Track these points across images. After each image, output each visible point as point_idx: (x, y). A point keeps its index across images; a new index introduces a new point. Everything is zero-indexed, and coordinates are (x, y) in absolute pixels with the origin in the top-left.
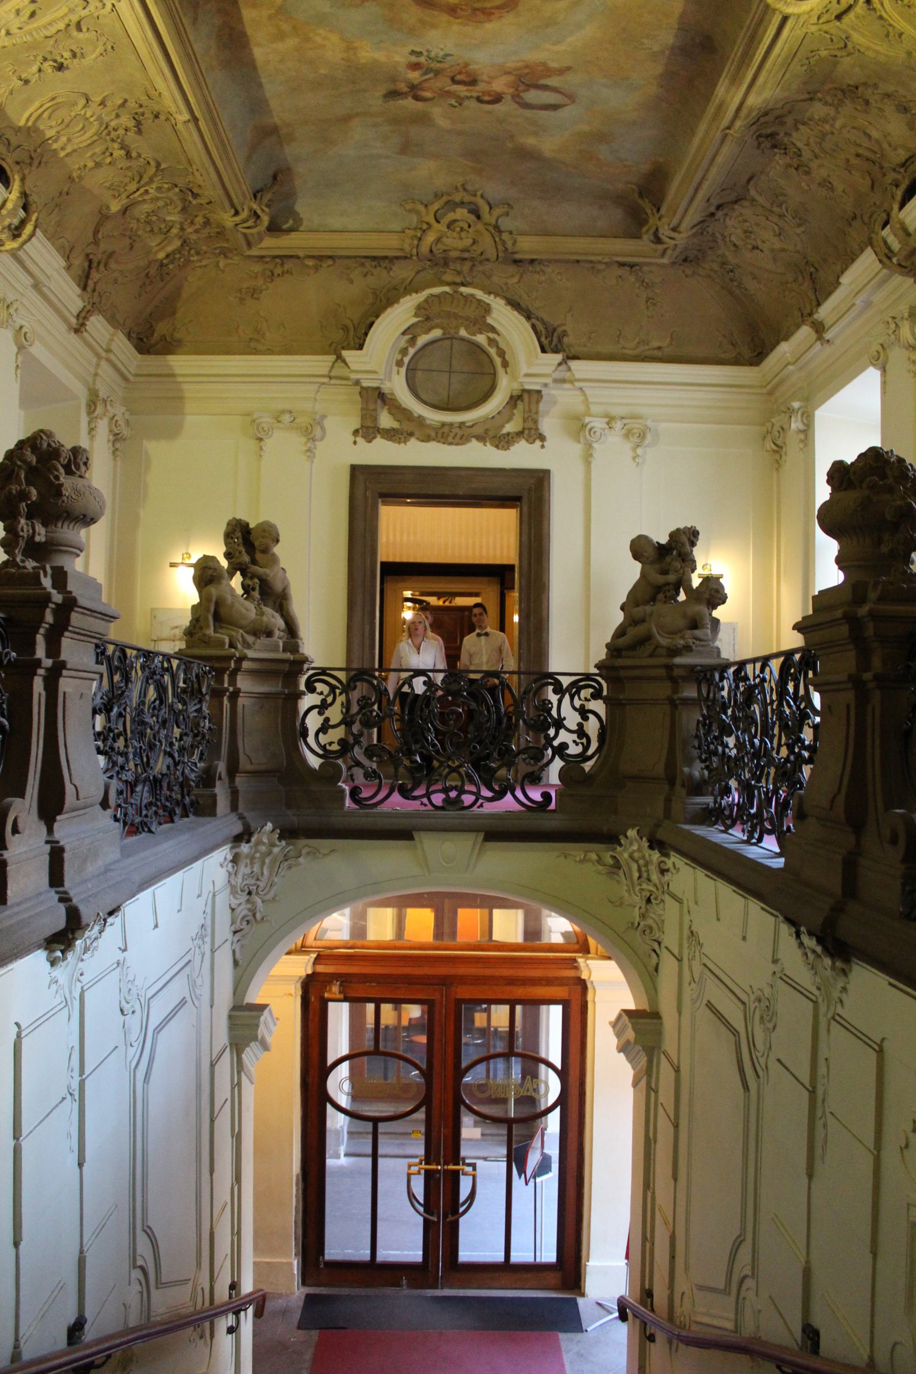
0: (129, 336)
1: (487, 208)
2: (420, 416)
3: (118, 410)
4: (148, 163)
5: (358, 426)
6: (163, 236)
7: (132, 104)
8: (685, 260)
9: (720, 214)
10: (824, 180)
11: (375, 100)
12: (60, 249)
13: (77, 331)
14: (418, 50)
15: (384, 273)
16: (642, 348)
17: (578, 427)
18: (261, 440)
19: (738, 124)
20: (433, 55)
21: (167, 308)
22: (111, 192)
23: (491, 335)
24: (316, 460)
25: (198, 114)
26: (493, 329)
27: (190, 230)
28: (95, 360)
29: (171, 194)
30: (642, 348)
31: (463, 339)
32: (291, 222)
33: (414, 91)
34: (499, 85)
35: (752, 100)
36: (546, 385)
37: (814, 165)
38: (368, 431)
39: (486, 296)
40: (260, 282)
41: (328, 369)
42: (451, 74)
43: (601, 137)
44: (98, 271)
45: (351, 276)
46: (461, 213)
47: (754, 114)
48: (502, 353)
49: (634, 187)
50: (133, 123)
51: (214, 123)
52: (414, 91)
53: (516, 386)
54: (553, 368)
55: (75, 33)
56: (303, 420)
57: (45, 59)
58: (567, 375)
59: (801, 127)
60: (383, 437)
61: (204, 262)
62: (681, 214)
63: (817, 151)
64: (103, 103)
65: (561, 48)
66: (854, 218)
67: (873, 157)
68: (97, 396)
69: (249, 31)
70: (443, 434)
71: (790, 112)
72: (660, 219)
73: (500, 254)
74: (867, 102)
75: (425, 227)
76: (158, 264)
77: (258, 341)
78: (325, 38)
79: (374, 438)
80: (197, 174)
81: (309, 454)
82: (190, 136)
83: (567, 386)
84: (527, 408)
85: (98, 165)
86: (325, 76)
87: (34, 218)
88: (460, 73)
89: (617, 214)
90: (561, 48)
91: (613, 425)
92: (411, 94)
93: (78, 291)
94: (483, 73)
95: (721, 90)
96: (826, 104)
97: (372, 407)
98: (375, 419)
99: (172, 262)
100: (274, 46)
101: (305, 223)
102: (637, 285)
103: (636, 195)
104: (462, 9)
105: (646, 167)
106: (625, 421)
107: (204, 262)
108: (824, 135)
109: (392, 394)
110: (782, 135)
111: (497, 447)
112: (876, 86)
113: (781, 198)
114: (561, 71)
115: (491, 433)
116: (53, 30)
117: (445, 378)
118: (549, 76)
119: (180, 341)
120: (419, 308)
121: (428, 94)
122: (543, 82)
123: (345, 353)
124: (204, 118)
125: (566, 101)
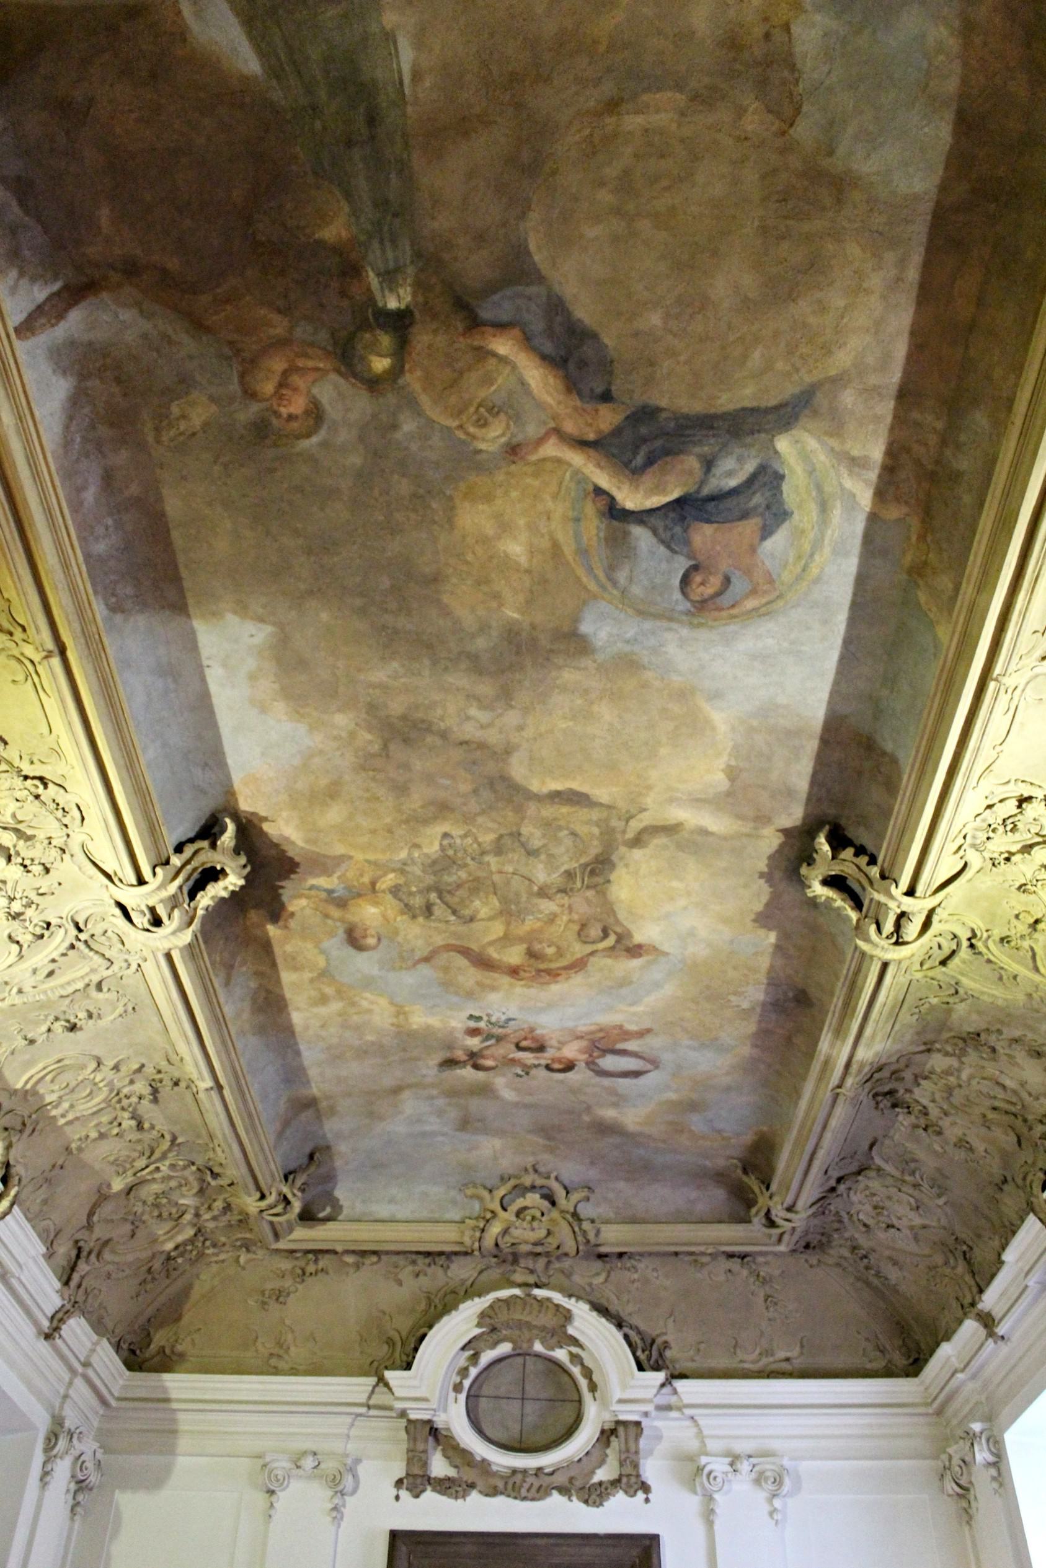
0: (118, 1348)
1: (564, 1193)
2: (484, 1460)
3: (88, 1446)
4: (163, 1136)
5: (402, 1474)
6: (171, 1224)
7: (149, 1070)
8: (807, 1246)
9: (842, 1188)
10: (961, 1140)
11: (429, 1068)
12: (43, 1235)
13: (48, 1337)
14: (477, 1014)
15: (440, 1272)
16: (765, 1360)
17: (692, 1472)
18: (272, 1492)
19: (849, 1081)
20: (493, 1019)
21: (171, 1313)
22: (114, 1168)
23: (575, 1350)
24: (343, 1524)
25: (222, 1081)
26: (575, 1342)
27: (207, 1216)
28: (66, 1376)
29: (187, 1173)
30: (765, 1360)
31: (538, 1356)
32: (328, 1210)
33: (474, 1059)
34: (571, 1051)
35: (862, 1054)
36: (646, 1414)
37: (945, 1123)
38: (415, 1481)
39: (566, 1299)
40: (288, 1283)
41: (367, 1395)
42: (515, 1040)
43: (693, 1106)
44: (87, 1262)
45: (400, 1276)
46: (533, 1199)
47: (866, 1069)
48: (588, 1373)
49: (735, 1161)
50: (149, 1090)
51: (241, 1092)
52: (474, 1059)
53: (608, 1417)
54: (655, 1391)
55: (93, 993)
56: (330, 1466)
57: (57, 1019)
58: (673, 1400)
59: (922, 1082)
60: (434, 1490)
61: (222, 1257)
62: (796, 1189)
63: (945, 1107)
64: (116, 1068)
65: (639, 1009)
66: (1005, 1181)
67: (1013, 1109)
68: (61, 1424)
69: (288, 994)
70: (514, 1485)
71: (907, 1066)
72: (771, 1198)
73: (581, 1248)
74: (994, 1050)
75: (489, 1215)
76: (164, 1257)
77: (279, 1356)
78: (372, 1003)
79: (423, 1491)
80: (218, 1150)
81: (334, 1514)
82: (212, 1105)
83: (674, 1414)
84: (623, 1446)
85: (102, 1136)
86: (373, 1043)
87: (13, 1192)
88: (525, 1039)
89: (719, 1194)
90: (639, 1009)
91: (738, 1466)
92: (471, 1062)
93: (58, 1285)
95: (824, 1045)
96: (947, 1054)
97: (420, 1446)
98: (425, 1464)
99: (182, 1255)
100: (315, 1010)
101: (345, 1211)
102: (752, 1280)
103: (739, 1171)
105: (748, 1138)
106: (753, 1460)
107: (222, 1257)
108: (949, 1091)
109: (448, 1429)
110: (901, 1091)
111: (586, 1502)
112: (999, 1032)
113: (913, 1165)
114: (641, 1034)
115: (578, 1484)
116: (70, 990)
117: (514, 1407)
118: (626, 1040)
119: (182, 1355)
120: (483, 1315)
121: (489, 1063)
123: (389, 1375)
124: (230, 1087)
125: (649, 1067)
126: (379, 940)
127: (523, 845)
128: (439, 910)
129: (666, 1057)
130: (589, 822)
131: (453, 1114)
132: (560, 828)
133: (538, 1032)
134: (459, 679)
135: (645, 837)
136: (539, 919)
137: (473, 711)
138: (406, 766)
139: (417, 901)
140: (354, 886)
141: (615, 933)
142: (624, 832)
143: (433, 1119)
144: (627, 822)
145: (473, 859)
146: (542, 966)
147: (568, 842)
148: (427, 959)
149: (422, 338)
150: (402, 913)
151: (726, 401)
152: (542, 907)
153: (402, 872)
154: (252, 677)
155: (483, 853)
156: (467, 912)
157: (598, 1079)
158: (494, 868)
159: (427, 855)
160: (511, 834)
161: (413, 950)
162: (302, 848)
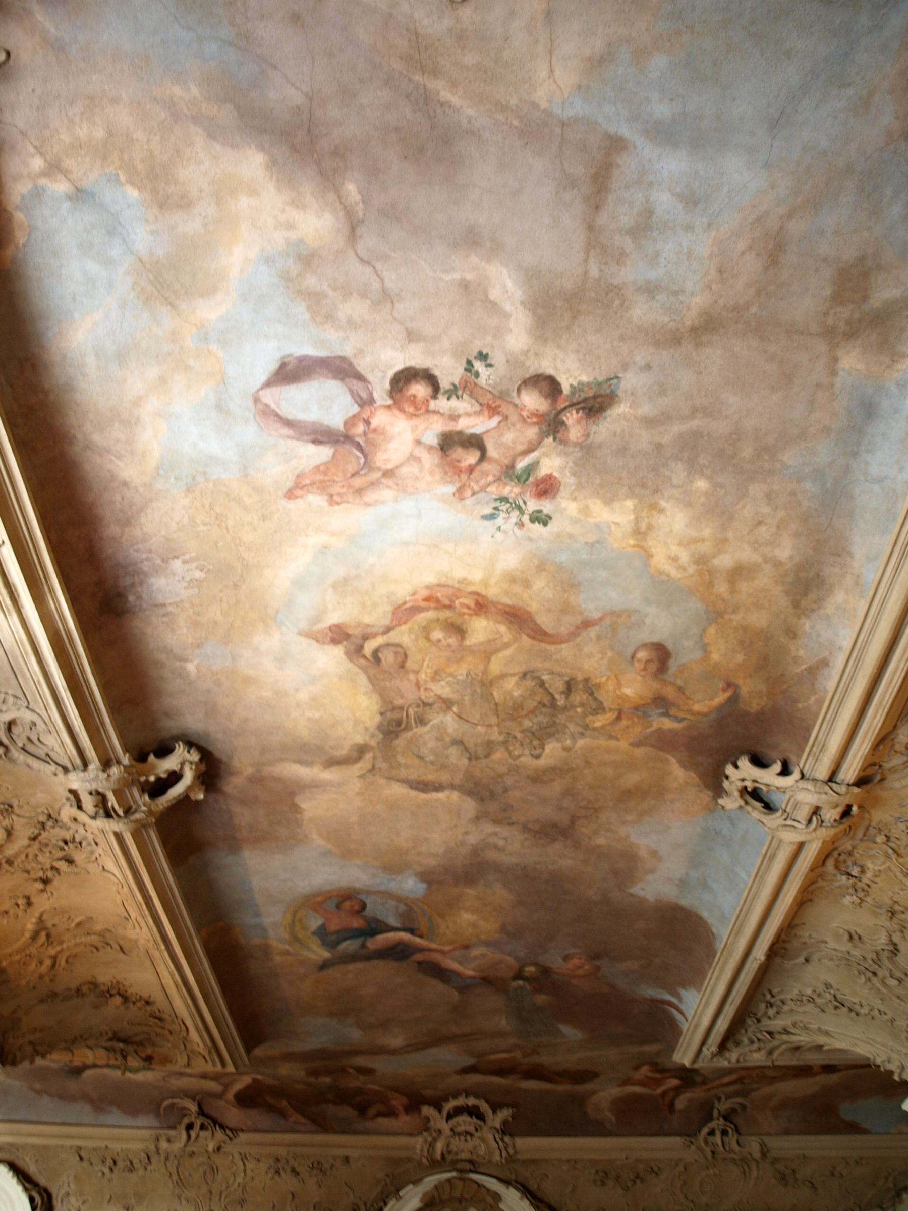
14: (537, 527)
42: (485, 466)
65: (315, 541)
88: (471, 469)
92: (561, 405)
94: (431, 473)
104: (469, 608)
122: (324, 453)
126: (633, 657)
127: (466, 750)
128: (558, 685)
129: (249, 432)
131: (620, 213)
132: (432, 763)
133: (450, 489)
134: (508, 860)
135: (355, 755)
136: (451, 675)
137: (501, 843)
138: (560, 808)
139: (578, 697)
140: (638, 717)
141: (365, 657)
142: (374, 758)
143: (664, 201)
144: (373, 768)
145: (515, 737)
146: (447, 614)
147: (424, 751)
148: (587, 624)
150: (598, 686)
151: (360, 965)
152: (448, 689)
153: (586, 727)
154: (652, 871)
155: (505, 743)
156: (529, 683)
157: (347, 351)
158: (496, 729)
159: (558, 740)
160: (477, 759)
161: (599, 638)
162: (673, 756)
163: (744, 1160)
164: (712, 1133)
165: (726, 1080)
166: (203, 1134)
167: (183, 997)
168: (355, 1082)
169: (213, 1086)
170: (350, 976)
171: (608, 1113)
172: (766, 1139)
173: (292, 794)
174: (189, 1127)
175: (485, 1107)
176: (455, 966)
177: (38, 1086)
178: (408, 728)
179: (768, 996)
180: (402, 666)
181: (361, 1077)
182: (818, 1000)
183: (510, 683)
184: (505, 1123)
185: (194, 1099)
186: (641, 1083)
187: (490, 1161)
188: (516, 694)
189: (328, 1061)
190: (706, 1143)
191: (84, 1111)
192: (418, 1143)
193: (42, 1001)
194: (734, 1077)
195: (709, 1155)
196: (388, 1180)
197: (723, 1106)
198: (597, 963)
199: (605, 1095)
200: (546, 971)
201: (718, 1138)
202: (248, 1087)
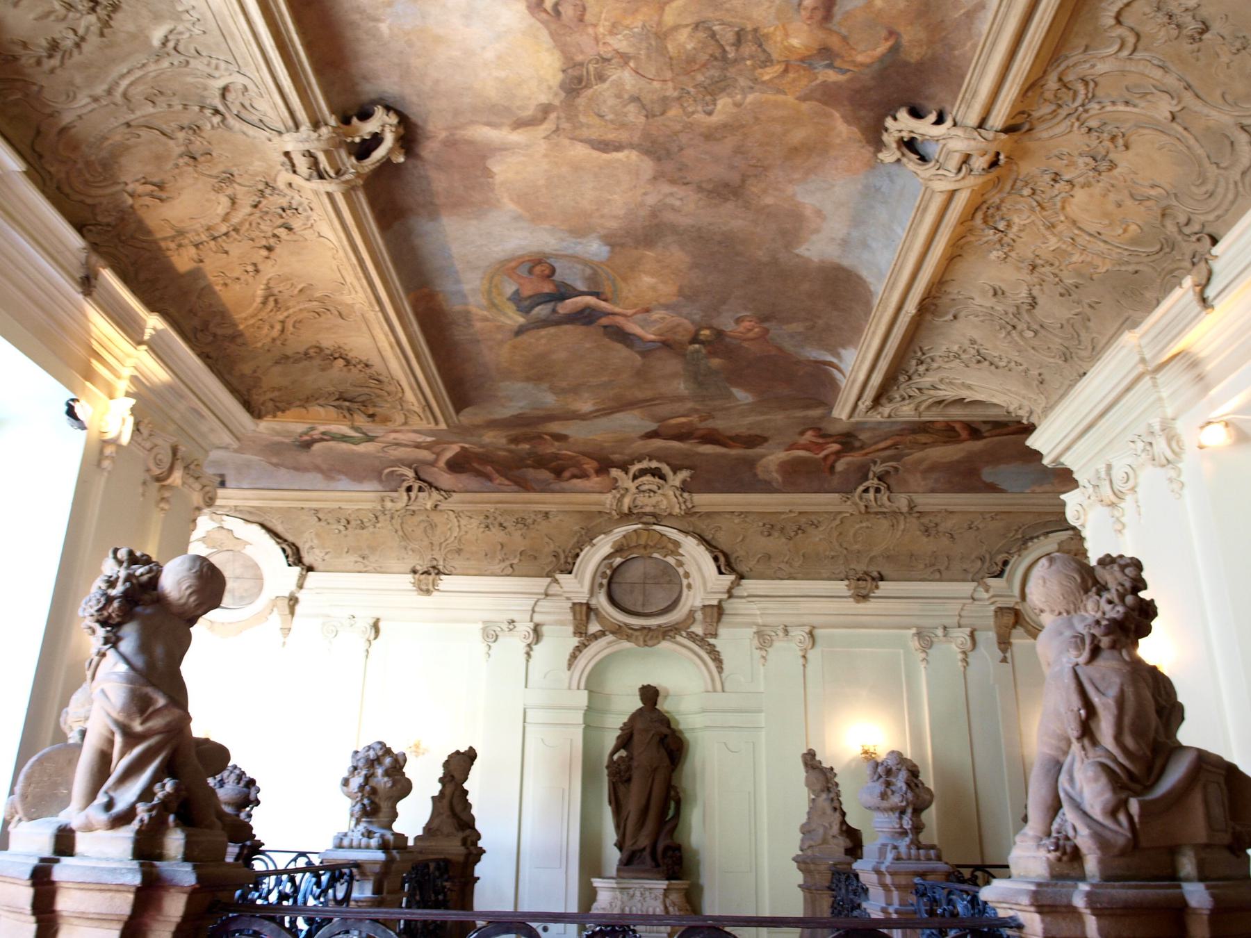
127: (644, 107)
128: (728, 36)
130: (589, 126)
132: (612, 122)
134: (684, 221)
135: (540, 115)
136: (627, 27)
137: (678, 203)
138: (732, 167)
139: (748, 49)
140: (805, 69)
141: (545, 11)
142: (558, 118)
144: (558, 129)
145: (688, 93)
147: (604, 110)
149: (687, 338)
150: (767, 36)
151: (552, 330)
152: (625, 43)
153: (755, 80)
154: (817, 231)
155: (679, 98)
156: (701, 35)
158: (670, 84)
159: (729, 95)
160: (654, 116)
163: (896, 514)
164: (866, 491)
165: (882, 445)
166: (421, 494)
167: (397, 358)
168: (551, 448)
169: (426, 455)
170: (543, 341)
171: (775, 475)
172: (914, 496)
173: (484, 158)
174: (409, 489)
175: (666, 469)
176: (636, 329)
177: (274, 460)
178: (588, 86)
179: (919, 354)
180: (581, 20)
181: (556, 444)
182: (964, 356)
183: (683, 36)
184: (684, 482)
185: (410, 467)
186: (805, 448)
187: (670, 514)
188: (689, 47)
189: (525, 426)
190: (861, 498)
191: (316, 479)
192: (608, 499)
193: (277, 363)
194: (889, 443)
195: (863, 509)
196: (583, 532)
197: (878, 469)
198: (766, 325)
199: (773, 458)
200: (720, 334)
201: (871, 495)
202: (457, 454)
